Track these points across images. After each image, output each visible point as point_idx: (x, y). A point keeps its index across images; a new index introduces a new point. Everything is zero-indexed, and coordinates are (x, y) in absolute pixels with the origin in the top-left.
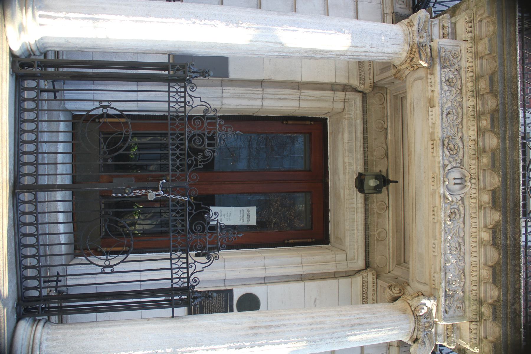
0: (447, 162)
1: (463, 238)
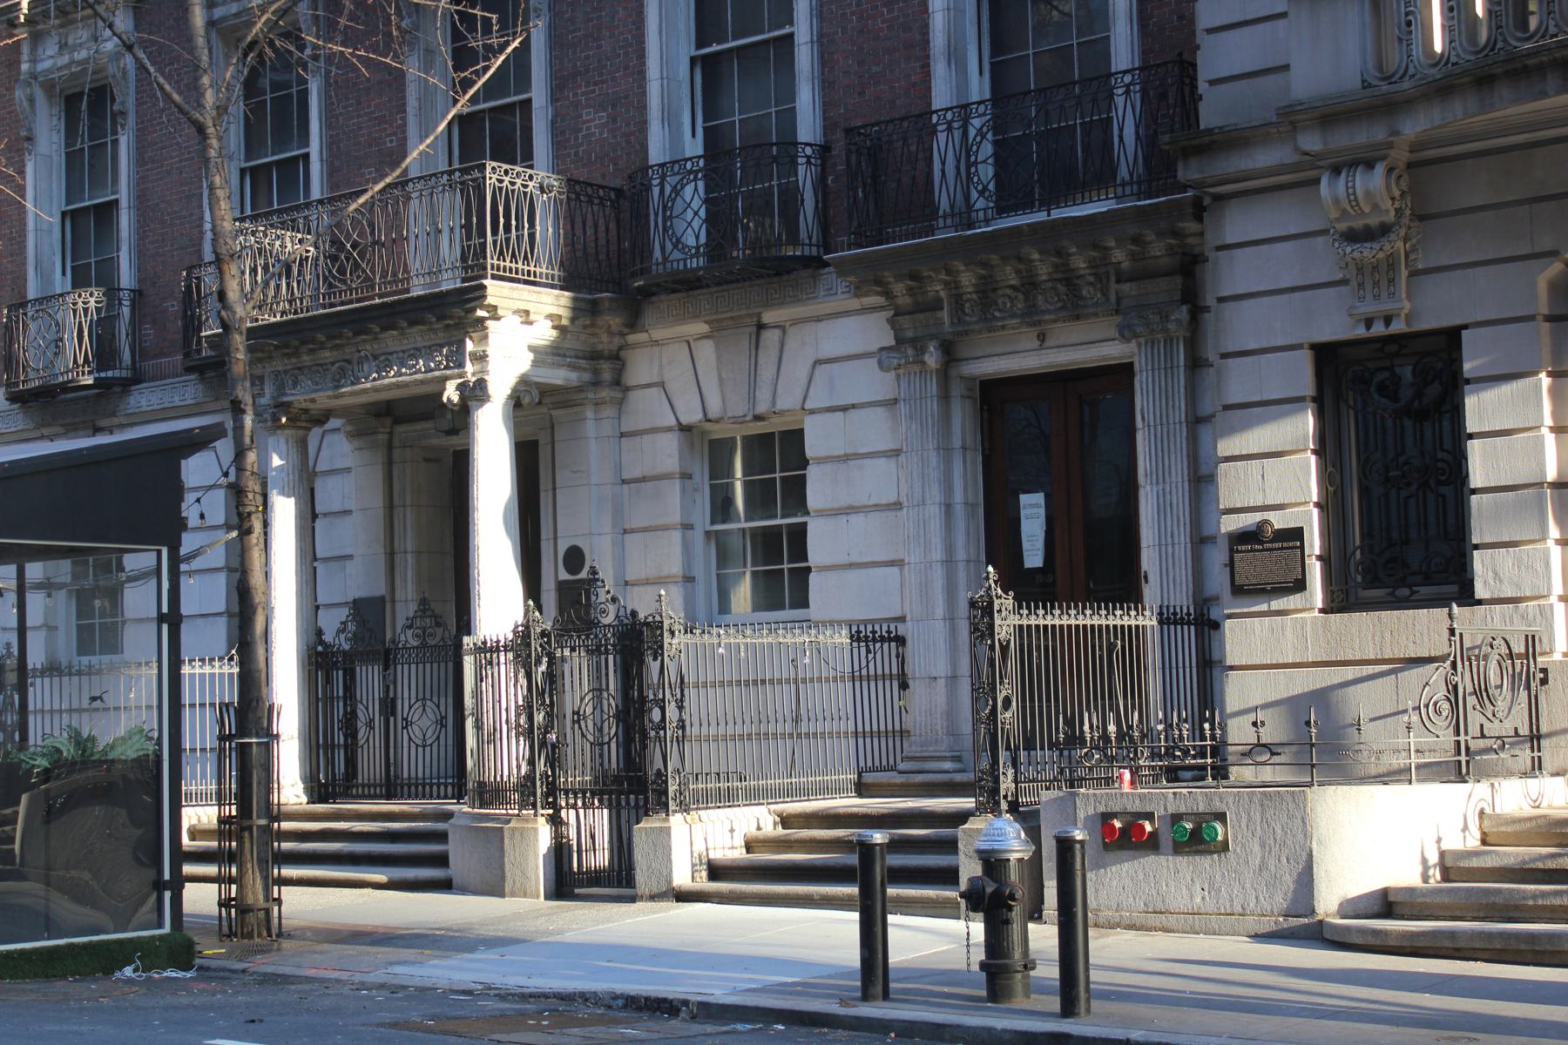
0: (349, 382)
1: (404, 352)
